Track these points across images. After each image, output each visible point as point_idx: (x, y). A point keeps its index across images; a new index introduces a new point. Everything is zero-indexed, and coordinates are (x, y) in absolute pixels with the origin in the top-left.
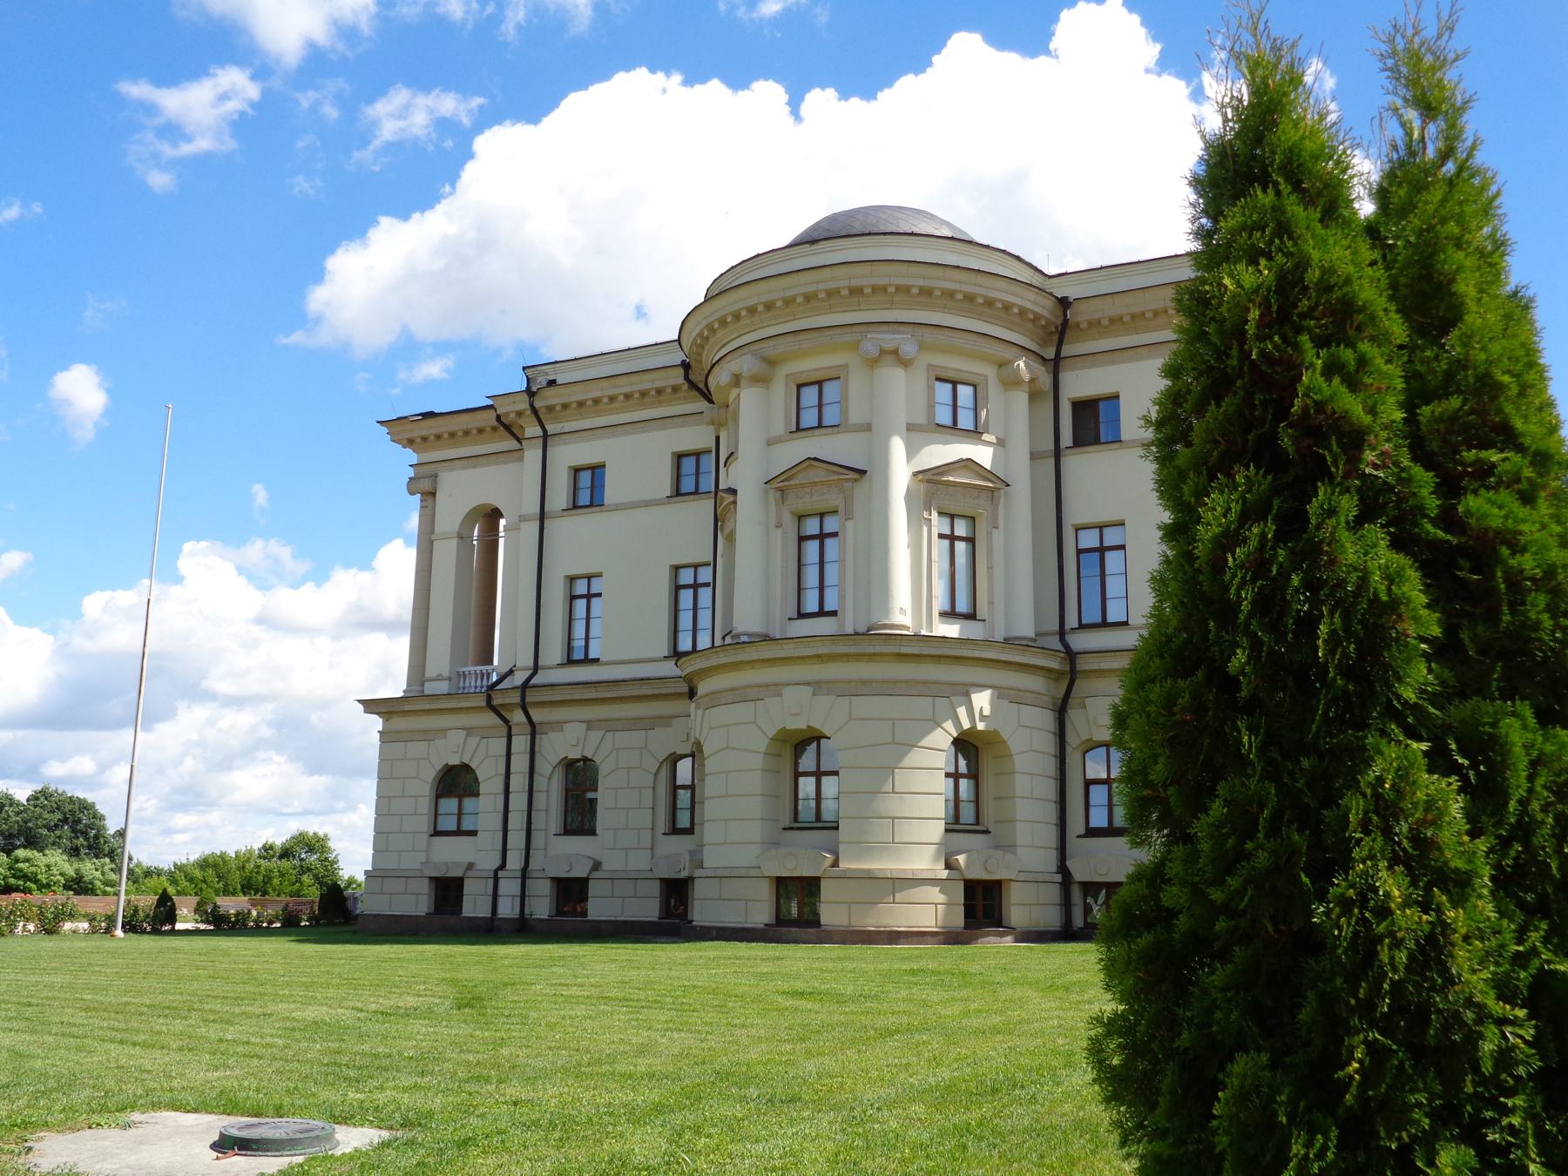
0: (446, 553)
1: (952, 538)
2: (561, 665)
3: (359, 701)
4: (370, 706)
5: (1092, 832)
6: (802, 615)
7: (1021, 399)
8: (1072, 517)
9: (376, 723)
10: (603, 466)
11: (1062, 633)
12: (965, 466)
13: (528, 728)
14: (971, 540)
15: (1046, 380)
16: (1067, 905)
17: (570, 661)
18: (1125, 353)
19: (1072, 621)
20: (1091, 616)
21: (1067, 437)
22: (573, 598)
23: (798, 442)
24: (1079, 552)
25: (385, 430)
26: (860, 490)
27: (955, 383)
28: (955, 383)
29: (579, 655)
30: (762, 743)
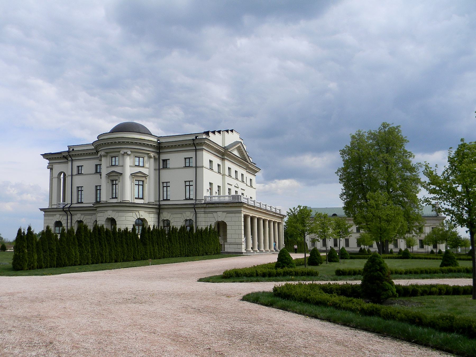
0: (55, 181)
1: (139, 185)
2: (76, 203)
3: (39, 209)
4: (41, 209)
6: (113, 198)
7: (152, 160)
9: (43, 213)
11: (159, 201)
13: (70, 215)
14: (143, 185)
15: (157, 156)
17: (78, 203)
18: (171, 152)
21: (161, 167)
22: (78, 191)
25: (42, 156)
26: (121, 177)
27: (139, 158)
28: (139, 158)
29: (80, 201)
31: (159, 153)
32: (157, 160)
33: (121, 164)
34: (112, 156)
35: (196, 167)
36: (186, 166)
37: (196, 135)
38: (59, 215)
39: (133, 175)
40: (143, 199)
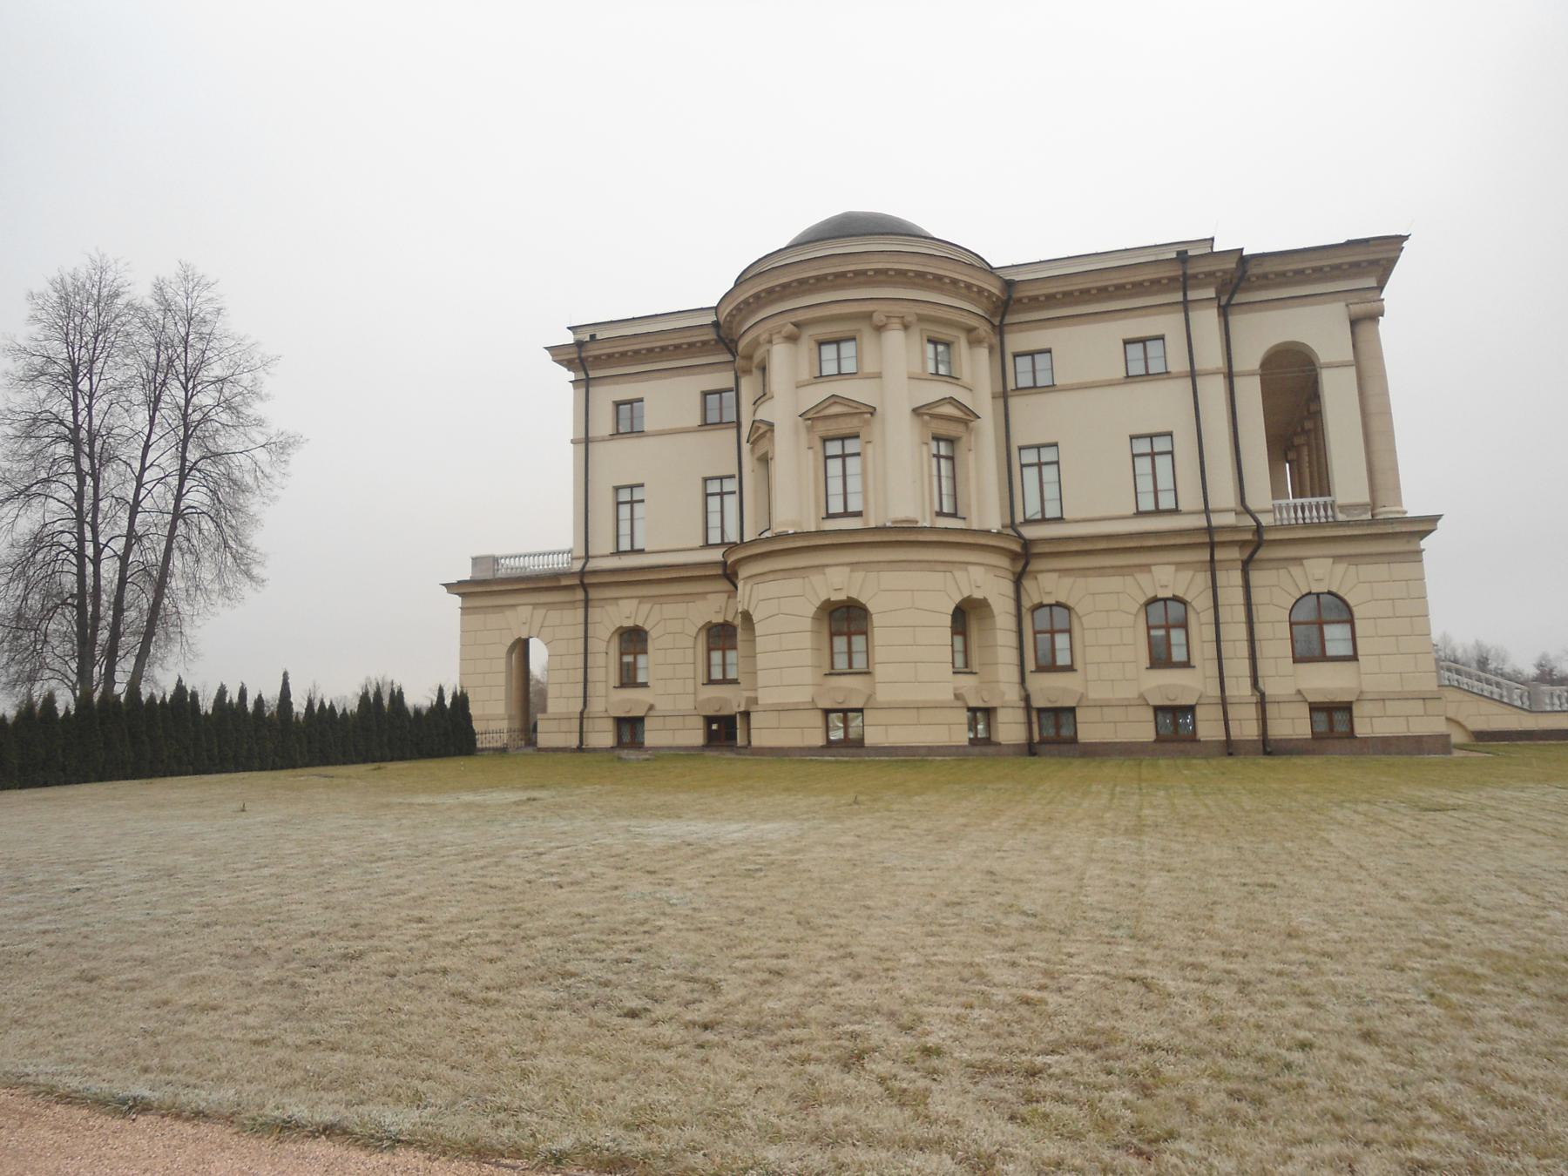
1: (938, 457)
5: (1040, 669)
6: (829, 516)
8: (1017, 441)
9: (457, 600)
10: (614, 402)
12: (950, 403)
15: (995, 340)
16: (1029, 723)
17: (618, 553)
19: (1019, 518)
20: (1033, 510)
22: (618, 503)
23: (819, 386)
24: (1022, 466)
30: (811, 610)
31: (1000, 330)
32: (998, 351)
33: (869, 367)
34: (821, 338)
35: (1193, 375)
36: (1128, 376)
37: (1182, 248)
38: (531, 607)
39: (927, 414)
40: (960, 514)
